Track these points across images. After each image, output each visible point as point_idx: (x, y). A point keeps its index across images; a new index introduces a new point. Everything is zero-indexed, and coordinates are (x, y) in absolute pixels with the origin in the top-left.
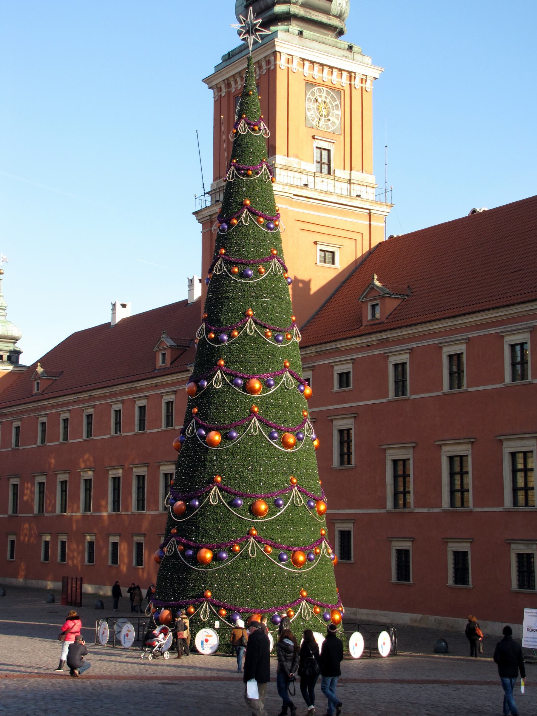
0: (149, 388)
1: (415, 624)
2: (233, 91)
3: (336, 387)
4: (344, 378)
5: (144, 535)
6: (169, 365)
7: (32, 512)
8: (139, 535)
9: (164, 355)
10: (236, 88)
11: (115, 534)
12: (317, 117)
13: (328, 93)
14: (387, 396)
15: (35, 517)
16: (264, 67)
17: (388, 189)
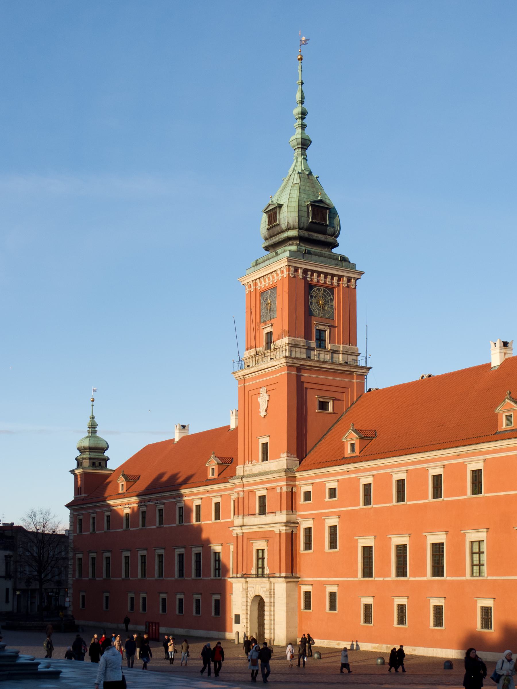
0: (203, 493)
1: (374, 650)
2: (259, 288)
3: (327, 499)
4: (333, 493)
5: (201, 594)
6: (217, 477)
7: (121, 576)
8: (197, 594)
9: (213, 469)
10: (261, 287)
11: (181, 593)
12: (317, 308)
13: (325, 291)
14: (359, 505)
15: (123, 580)
16: (280, 275)
17: (368, 356)
